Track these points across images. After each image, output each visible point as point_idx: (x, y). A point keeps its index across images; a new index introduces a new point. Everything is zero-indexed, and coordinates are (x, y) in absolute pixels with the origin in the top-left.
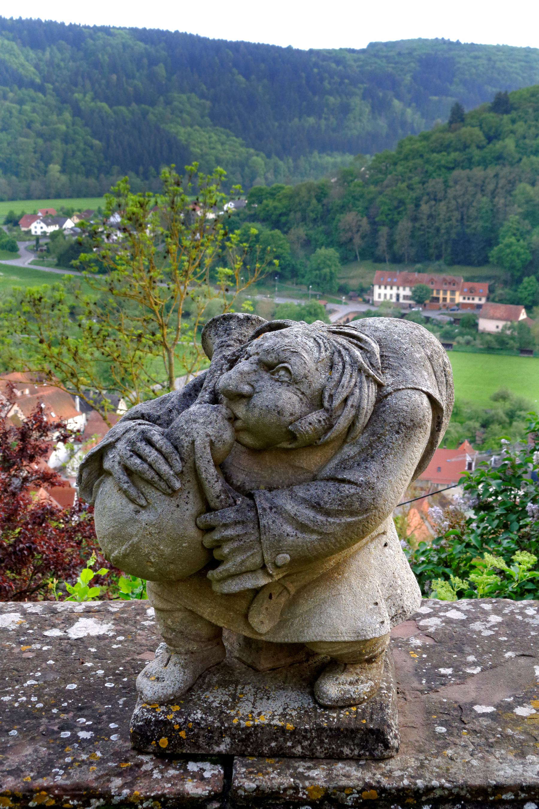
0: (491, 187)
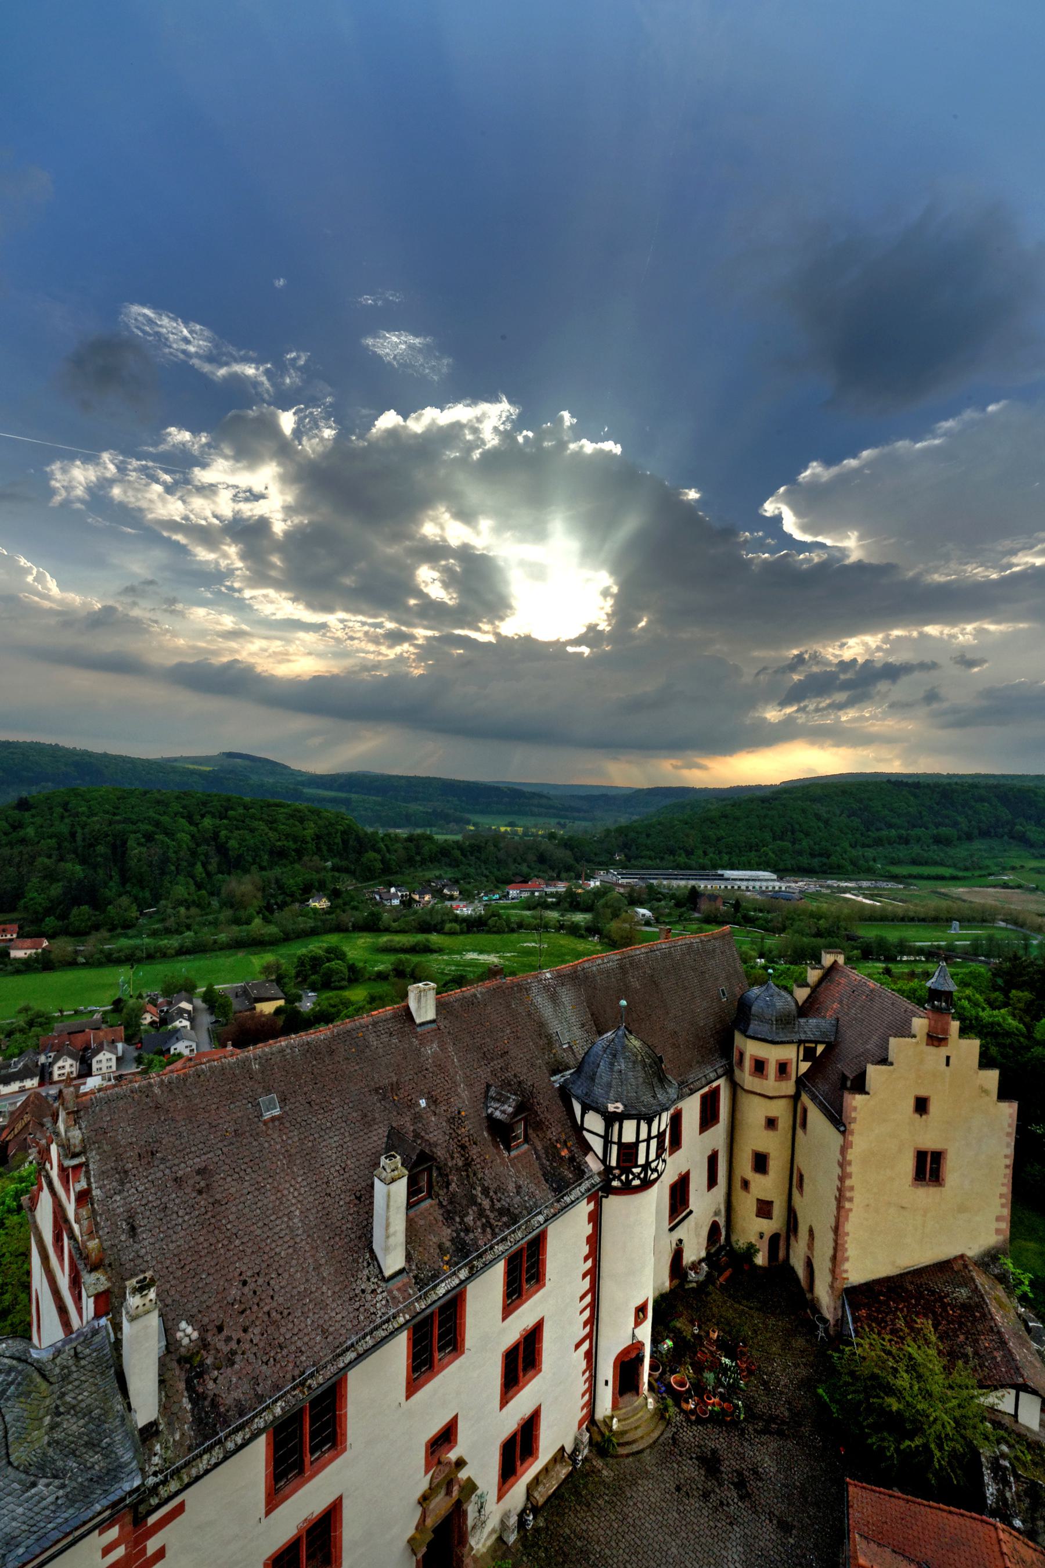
0: (17, 860)
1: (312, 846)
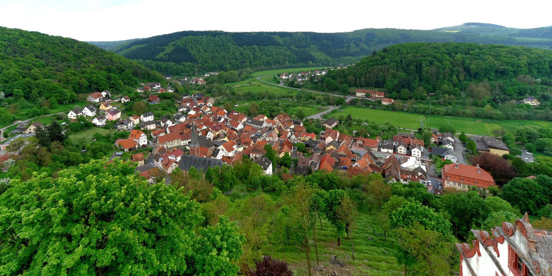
1: (525, 69)
